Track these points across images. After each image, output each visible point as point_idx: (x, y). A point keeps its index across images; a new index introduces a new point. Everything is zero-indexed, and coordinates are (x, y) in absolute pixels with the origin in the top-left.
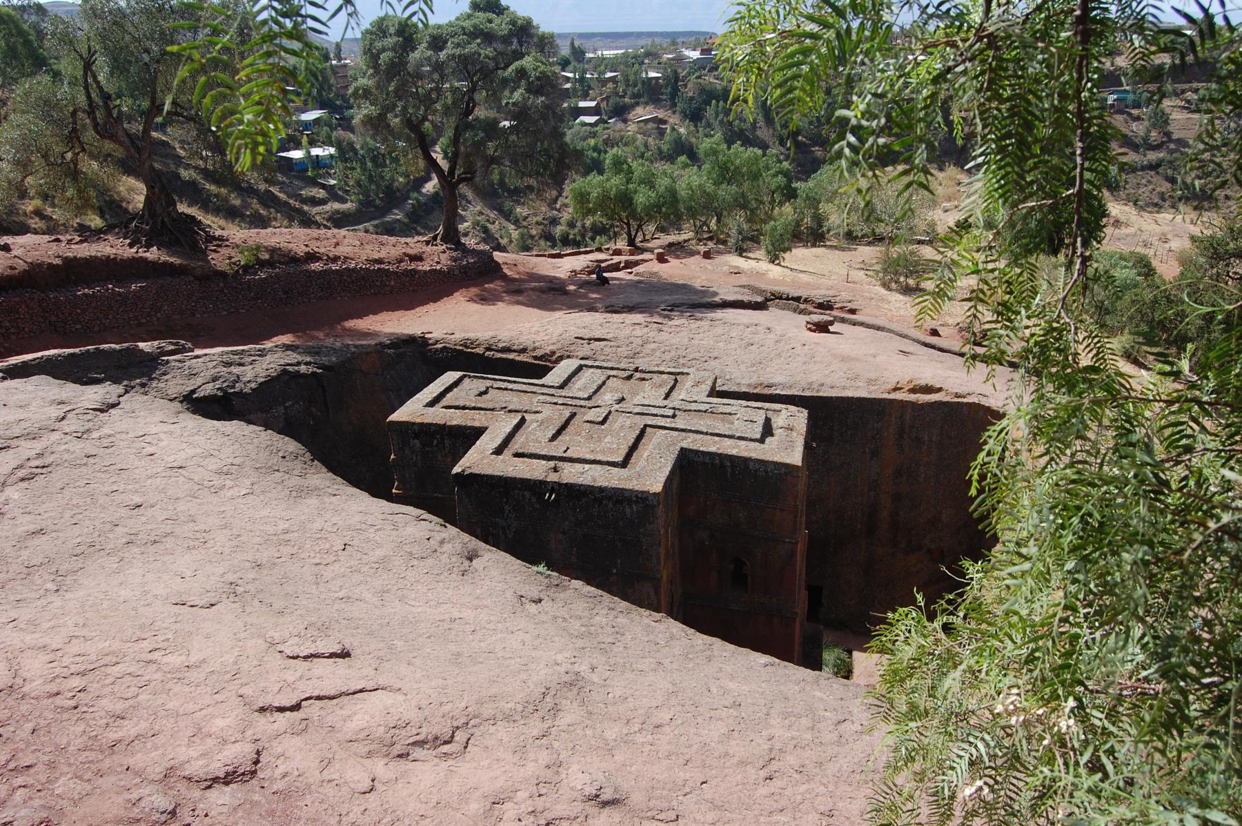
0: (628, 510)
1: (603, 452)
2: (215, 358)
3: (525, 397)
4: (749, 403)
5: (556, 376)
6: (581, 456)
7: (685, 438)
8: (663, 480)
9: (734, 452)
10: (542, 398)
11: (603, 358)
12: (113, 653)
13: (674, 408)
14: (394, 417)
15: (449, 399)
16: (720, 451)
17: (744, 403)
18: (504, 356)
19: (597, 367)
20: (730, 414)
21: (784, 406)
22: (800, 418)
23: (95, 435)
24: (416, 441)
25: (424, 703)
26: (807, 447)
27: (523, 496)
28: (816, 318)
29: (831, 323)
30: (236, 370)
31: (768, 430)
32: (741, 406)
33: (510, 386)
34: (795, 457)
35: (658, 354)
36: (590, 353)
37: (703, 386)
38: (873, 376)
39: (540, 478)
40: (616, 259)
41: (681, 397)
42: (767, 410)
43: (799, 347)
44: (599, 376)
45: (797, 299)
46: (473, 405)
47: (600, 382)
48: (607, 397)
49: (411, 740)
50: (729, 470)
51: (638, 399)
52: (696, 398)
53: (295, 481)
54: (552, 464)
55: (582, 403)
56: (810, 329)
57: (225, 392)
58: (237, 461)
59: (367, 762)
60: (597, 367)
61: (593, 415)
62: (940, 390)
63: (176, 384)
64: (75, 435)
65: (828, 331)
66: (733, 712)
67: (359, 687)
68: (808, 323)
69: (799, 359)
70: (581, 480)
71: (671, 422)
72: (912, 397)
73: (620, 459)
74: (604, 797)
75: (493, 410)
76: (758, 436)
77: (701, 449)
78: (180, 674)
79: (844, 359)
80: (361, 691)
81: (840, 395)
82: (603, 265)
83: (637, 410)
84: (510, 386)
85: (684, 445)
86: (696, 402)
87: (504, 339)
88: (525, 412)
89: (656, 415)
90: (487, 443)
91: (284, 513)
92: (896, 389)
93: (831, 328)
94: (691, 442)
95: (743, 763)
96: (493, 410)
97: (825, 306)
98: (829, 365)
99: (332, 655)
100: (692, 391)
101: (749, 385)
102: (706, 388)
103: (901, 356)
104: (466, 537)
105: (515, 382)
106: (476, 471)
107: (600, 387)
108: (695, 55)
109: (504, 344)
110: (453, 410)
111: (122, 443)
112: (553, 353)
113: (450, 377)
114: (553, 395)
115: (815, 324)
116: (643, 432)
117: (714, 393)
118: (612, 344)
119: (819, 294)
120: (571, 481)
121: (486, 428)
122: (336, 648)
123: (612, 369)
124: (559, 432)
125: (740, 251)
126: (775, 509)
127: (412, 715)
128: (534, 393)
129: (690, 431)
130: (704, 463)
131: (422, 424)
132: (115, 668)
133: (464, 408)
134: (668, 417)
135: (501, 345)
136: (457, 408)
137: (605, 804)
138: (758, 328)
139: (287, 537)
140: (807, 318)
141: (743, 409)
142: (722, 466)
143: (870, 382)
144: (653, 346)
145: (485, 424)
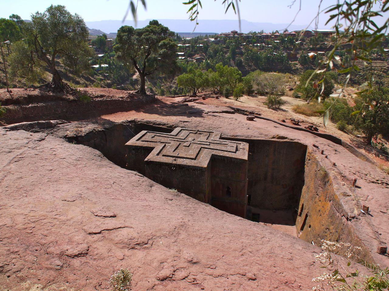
0: (196, 172)
1: (189, 155)
2: (73, 125)
3: (166, 138)
4: (232, 141)
5: (174, 132)
6: (183, 156)
7: (213, 151)
8: (207, 164)
9: (228, 156)
10: (170, 139)
11: (188, 127)
12: (44, 216)
13: (209, 142)
14: (127, 144)
15: (143, 139)
16: (224, 155)
17: (230, 141)
18: (159, 126)
19: (187, 130)
20: (226, 144)
21: (242, 142)
22: (246, 146)
23: (38, 148)
24: (133, 151)
25: (139, 232)
26: (249, 154)
27: (166, 168)
28: (250, 116)
29: (254, 118)
30: (80, 129)
31: (237, 150)
32: (229, 142)
33: (161, 135)
34: (246, 157)
35: (204, 126)
36: (184, 126)
37: (218, 136)
38: (266, 133)
39: (171, 163)
40: (191, 98)
41: (211, 139)
42: (237, 143)
43: (245, 125)
44: (187, 132)
45: (243, 111)
46: (150, 140)
47: (187, 134)
48: (190, 139)
49: (135, 243)
50: (226, 161)
51: (199, 140)
52: (216, 140)
53: (98, 163)
55: (182, 140)
56: (248, 120)
57: (77, 136)
58: (81, 157)
59: (122, 250)
60: (187, 130)
61: (185, 144)
62: (286, 138)
63: (61, 133)
64: (32, 148)
65: (253, 121)
66: (231, 234)
67: (119, 227)
68: (247, 118)
69: (245, 128)
70: (183, 163)
71: (209, 147)
72: (278, 140)
73: (194, 157)
74: (194, 261)
75: (156, 142)
76: (235, 151)
77: (218, 155)
78: (64, 223)
79: (258, 128)
80: (120, 228)
82: (187, 100)
83: (199, 143)
84: (161, 135)
85: (213, 153)
86: (216, 140)
87: (159, 121)
88: (166, 143)
89: (204, 144)
90: (155, 152)
91: (95, 173)
92: (273, 138)
93: (254, 120)
94: (214, 152)
95: (235, 250)
96: (156, 142)
97: (251, 113)
98: (254, 130)
99: (111, 217)
100: (215, 137)
101: (230, 136)
102: (219, 137)
104: (150, 180)
105: (163, 134)
107: (187, 136)
108: (213, 39)
109: (159, 123)
110: (144, 142)
111: (46, 151)
112: (173, 125)
113: (144, 132)
114: (174, 138)
115: (249, 118)
116: (200, 149)
117: (221, 138)
119: (250, 110)
121: (154, 147)
122: (112, 214)
123: (191, 130)
124: (176, 149)
125: (227, 97)
127: (135, 235)
128: (169, 137)
132: (45, 220)
133: (148, 141)
134: (208, 145)
135: (158, 123)
136: (146, 141)
137: (195, 263)
138: (233, 119)
139: (96, 180)
140: (247, 116)
141: (230, 143)
142: (224, 160)
143: (266, 135)
144: (202, 124)
145: (154, 146)
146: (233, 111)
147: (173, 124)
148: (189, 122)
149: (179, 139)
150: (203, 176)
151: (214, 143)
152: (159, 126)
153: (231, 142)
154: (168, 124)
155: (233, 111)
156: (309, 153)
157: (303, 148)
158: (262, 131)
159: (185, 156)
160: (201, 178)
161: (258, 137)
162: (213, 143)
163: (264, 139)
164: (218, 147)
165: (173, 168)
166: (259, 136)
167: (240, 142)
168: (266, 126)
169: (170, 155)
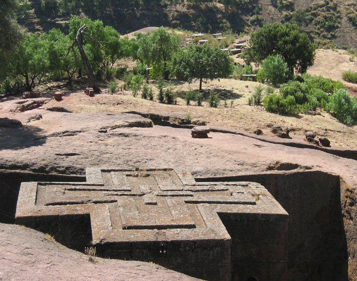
18: (13, 171)
33: (78, 187)
38: (253, 161)
39: (154, 240)
43: (200, 148)
56: (196, 137)
62: (296, 166)
65: (207, 137)
70: (180, 238)
75: (82, 203)
77: (228, 212)
79: (230, 153)
83: (169, 193)
87: (10, 159)
92: (270, 168)
93: (209, 135)
94: (220, 208)
103: (257, 148)
106: (111, 240)
109: (11, 163)
110: (58, 206)
112: (47, 166)
118: (80, 156)
129: (214, 202)
143: (254, 165)
144: (108, 155)
145: (86, 212)
146: (148, 120)
147: (45, 162)
148: (78, 154)
149: (123, 190)
151: (198, 191)
152: (13, 171)
153: (227, 185)
154: (33, 164)
155: (148, 120)
156: (348, 190)
157: (336, 181)
158: (241, 158)
160: (220, 264)
161: (239, 170)
162: (196, 191)
163: (251, 174)
165: (163, 252)
166: (239, 167)
168: (242, 147)
169: (139, 224)
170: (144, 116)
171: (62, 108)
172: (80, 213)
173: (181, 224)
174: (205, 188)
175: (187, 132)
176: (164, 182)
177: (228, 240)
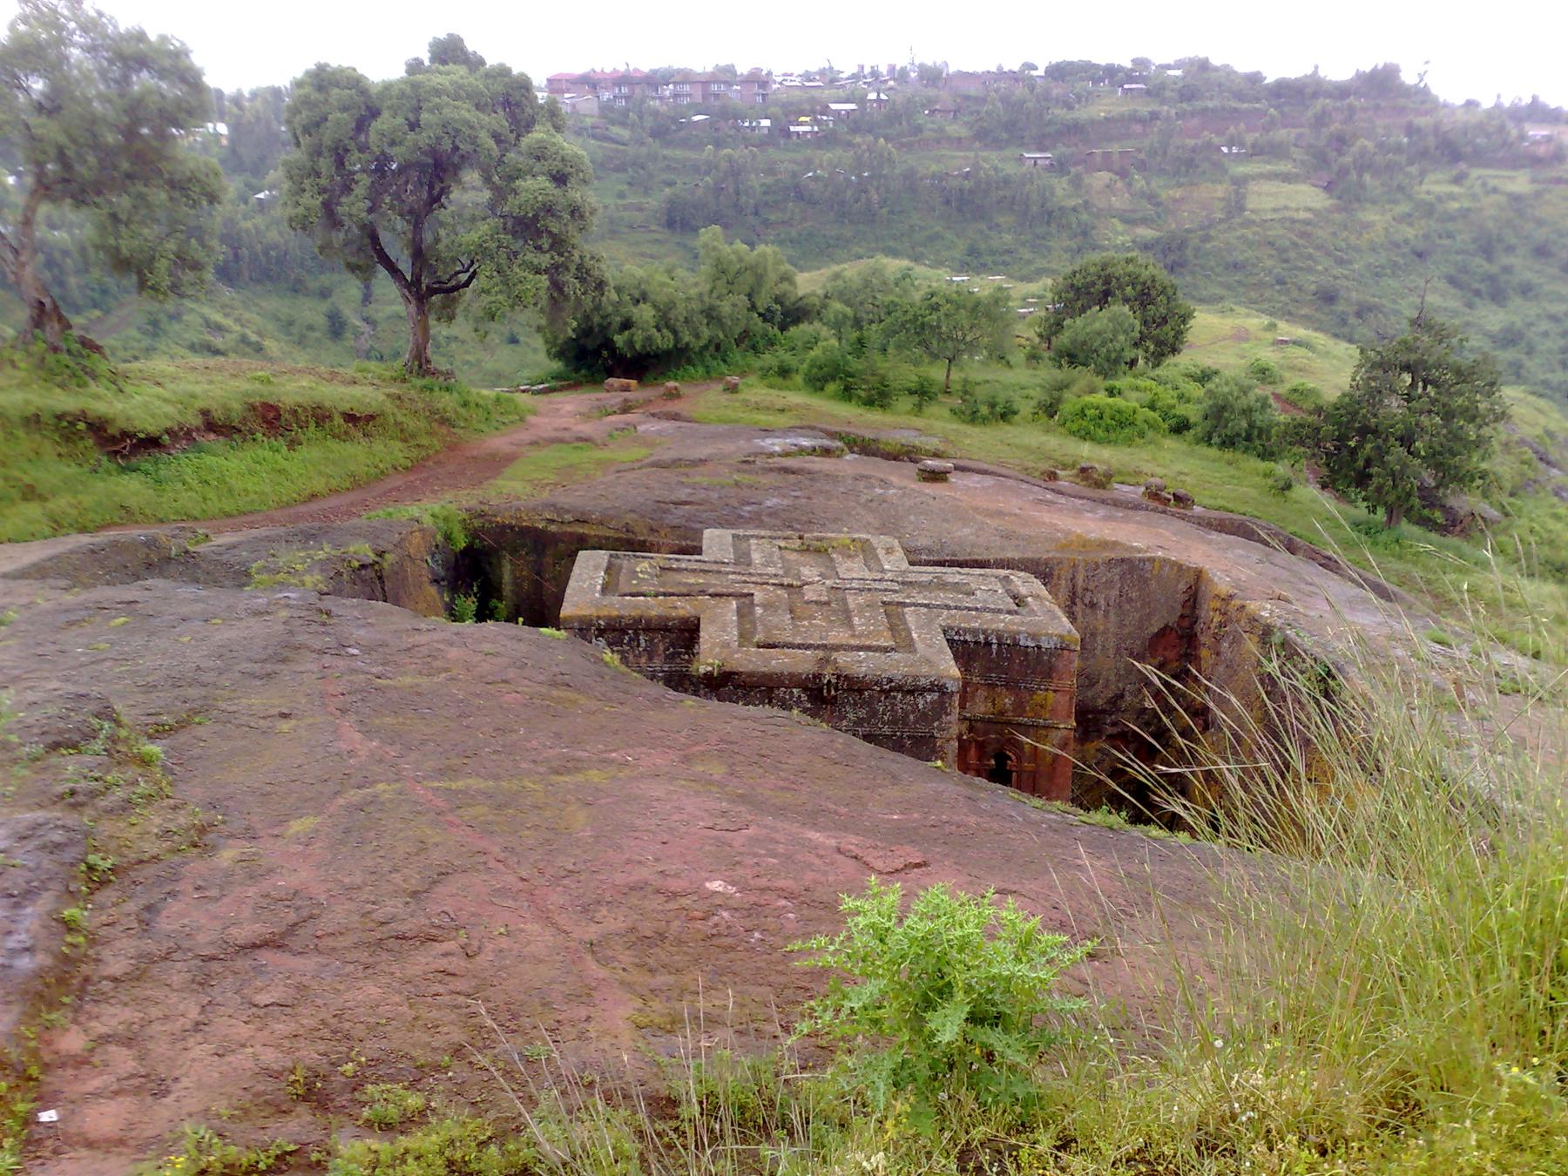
8: (953, 662)
54: (821, 654)
56: (925, 479)
62: (1115, 543)
71: (908, 597)
81: (999, 557)
85: (940, 621)
94: (944, 618)
105: (677, 560)
118: (701, 508)
120: (852, 672)
121: (699, 619)
126: (1047, 690)
130: (966, 642)
131: (609, 618)
134: (895, 591)
142: (988, 644)
150: (947, 715)
159: (853, 642)
164: (942, 597)
167: (1006, 572)
170: (832, 435)
171: (676, 414)
172: (682, 613)
173: (868, 643)
174: (925, 578)
175: (910, 469)
176: (849, 564)
177: (954, 679)
